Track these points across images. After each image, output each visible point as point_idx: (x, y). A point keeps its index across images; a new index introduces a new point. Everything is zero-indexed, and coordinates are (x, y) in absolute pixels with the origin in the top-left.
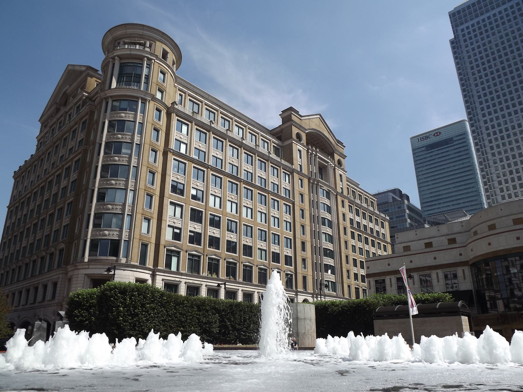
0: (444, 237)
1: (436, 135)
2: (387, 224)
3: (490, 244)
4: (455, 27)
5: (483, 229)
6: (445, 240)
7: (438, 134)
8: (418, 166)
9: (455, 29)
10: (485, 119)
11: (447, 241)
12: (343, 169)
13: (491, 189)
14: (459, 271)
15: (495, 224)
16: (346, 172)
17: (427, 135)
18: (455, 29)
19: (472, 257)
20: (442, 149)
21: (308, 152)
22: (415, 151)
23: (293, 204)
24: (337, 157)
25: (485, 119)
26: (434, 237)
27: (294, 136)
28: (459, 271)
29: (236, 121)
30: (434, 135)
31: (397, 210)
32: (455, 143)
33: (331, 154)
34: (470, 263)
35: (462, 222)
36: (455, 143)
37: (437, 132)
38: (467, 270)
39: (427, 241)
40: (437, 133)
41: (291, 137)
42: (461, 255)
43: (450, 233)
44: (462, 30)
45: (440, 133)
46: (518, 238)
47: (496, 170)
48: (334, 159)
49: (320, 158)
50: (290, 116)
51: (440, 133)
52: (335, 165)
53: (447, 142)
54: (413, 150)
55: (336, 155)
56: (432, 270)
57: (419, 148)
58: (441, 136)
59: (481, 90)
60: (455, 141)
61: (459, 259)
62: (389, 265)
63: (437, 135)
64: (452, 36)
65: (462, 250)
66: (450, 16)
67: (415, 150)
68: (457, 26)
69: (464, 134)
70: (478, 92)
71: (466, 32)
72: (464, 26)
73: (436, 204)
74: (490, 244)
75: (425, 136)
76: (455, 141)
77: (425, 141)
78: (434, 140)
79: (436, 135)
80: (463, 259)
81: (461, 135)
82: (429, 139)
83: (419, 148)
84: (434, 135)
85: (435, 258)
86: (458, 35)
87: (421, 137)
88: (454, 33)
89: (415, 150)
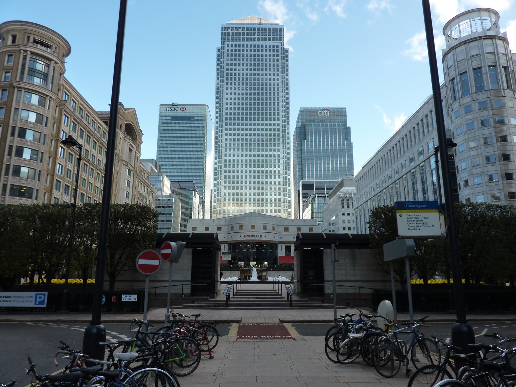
4: (224, 39)
9: (223, 41)
10: (227, 121)
11: (217, 229)
18: (223, 41)
22: (162, 117)
24: (138, 143)
25: (227, 121)
29: (87, 111)
30: (181, 109)
32: (195, 122)
36: (195, 122)
37: (183, 108)
44: (228, 46)
45: (186, 109)
49: (130, 144)
51: (186, 109)
58: (186, 111)
60: (196, 120)
67: (162, 116)
68: (225, 39)
69: (204, 117)
71: (230, 48)
72: (230, 43)
76: (196, 120)
77: (172, 111)
78: (178, 113)
80: (225, 240)
81: (201, 117)
89: (162, 116)
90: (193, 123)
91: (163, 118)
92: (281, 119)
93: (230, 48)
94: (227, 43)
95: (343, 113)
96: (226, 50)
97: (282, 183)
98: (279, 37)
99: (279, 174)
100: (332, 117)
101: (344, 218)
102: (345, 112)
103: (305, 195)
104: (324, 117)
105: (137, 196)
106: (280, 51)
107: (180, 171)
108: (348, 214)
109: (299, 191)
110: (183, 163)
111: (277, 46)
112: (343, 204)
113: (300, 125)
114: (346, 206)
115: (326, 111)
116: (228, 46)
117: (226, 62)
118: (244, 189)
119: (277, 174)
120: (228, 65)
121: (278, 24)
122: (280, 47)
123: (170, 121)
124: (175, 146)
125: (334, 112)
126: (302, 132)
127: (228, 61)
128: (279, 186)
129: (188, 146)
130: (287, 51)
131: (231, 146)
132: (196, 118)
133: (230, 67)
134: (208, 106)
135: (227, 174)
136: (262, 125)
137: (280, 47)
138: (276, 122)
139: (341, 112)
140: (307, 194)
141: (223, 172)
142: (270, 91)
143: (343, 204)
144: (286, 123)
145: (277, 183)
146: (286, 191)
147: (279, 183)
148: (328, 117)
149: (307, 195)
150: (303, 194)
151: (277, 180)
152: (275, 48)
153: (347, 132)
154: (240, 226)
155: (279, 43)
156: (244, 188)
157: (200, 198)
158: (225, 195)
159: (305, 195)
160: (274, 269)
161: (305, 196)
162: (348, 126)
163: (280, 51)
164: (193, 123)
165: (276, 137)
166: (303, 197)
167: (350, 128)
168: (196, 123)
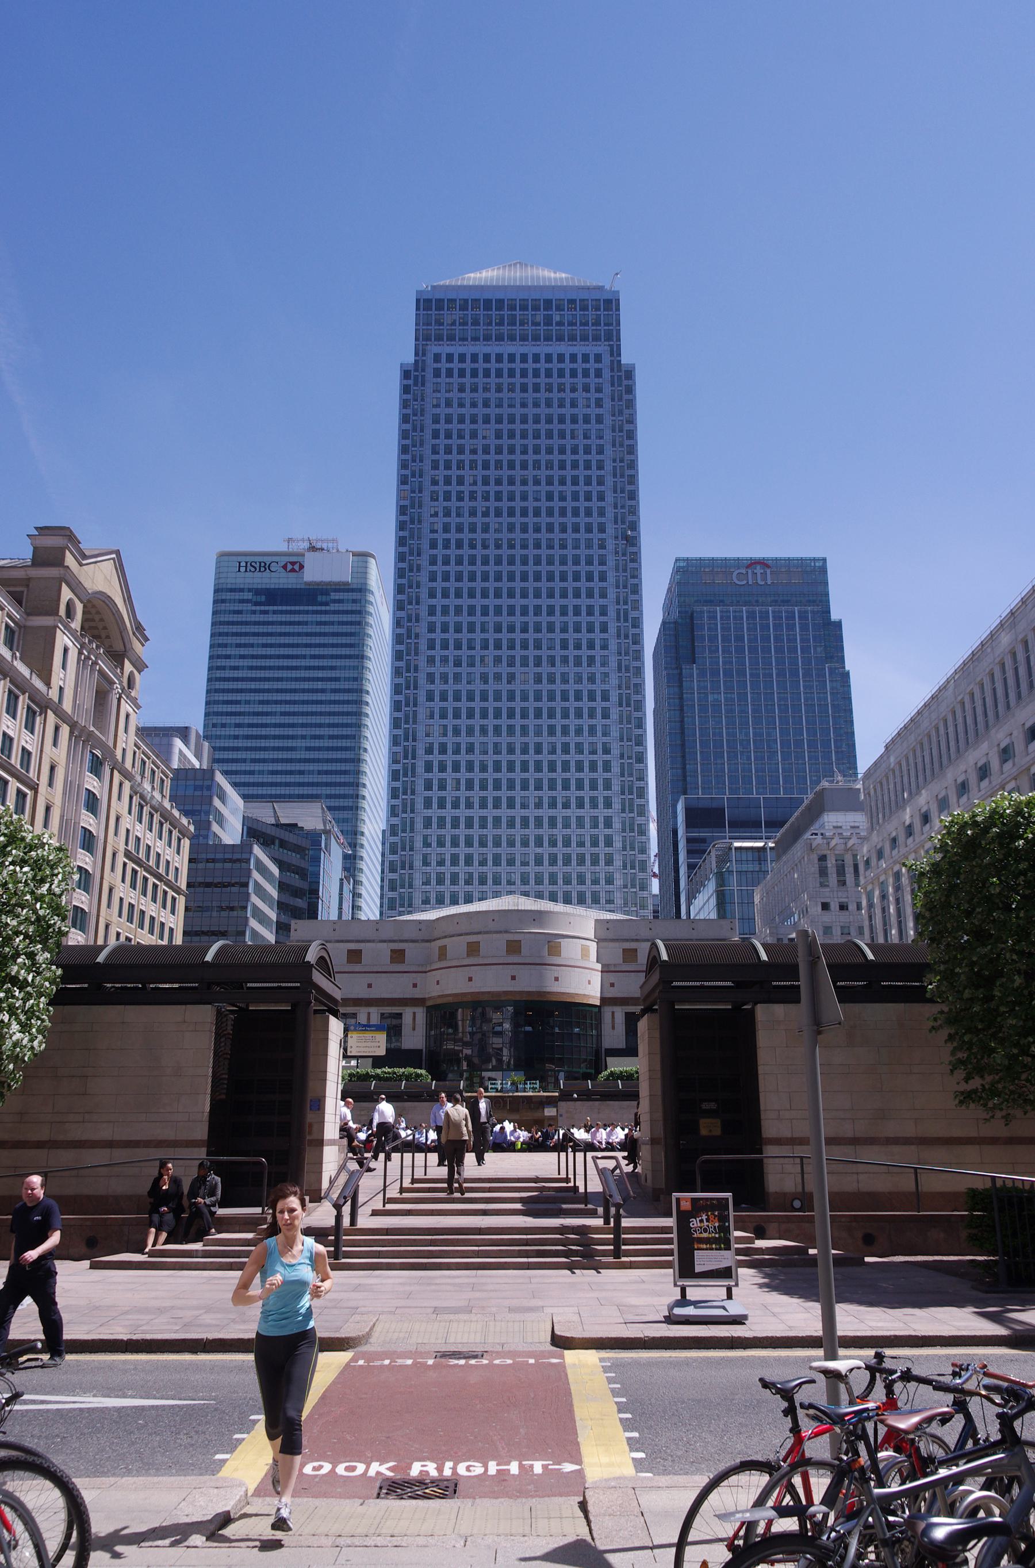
1: (290, 567)
2: (186, 843)
3: (470, 979)
4: (422, 338)
5: (457, 947)
6: (386, 949)
7: (297, 567)
8: (221, 640)
9: (421, 342)
10: (433, 602)
12: (134, 701)
13: (405, 775)
14: (408, 1013)
16: (139, 707)
17: (268, 560)
19: (434, 994)
20: (291, 612)
21: (80, 653)
22: (222, 594)
23: (35, 788)
24: (128, 667)
25: (433, 602)
26: (369, 941)
27: (62, 611)
28: (408, 1013)
30: (285, 567)
31: (190, 792)
32: (333, 607)
33: (117, 657)
34: (430, 1003)
35: (420, 922)
36: (333, 607)
38: (421, 1013)
39: (353, 946)
40: (293, 563)
41: (55, 612)
42: (415, 985)
44: (437, 358)
46: (513, 978)
47: (427, 735)
48: (122, 669)
50: (61, 552)
52: (123, 689)
53: (314, 595)
54: (217, 591)
55: (127, 663)
56: (360, 1005)
57: (232, 590)
59: (439, 527)
60: (335, 601)
61: (410, 993)
63: (293, 570)
64: (410, 358)
65: (418, 978)
66: (418, 301)
68: (427, 338)
69: (360, 590)
70: (433, 531)
72: (445, 349)
73: (244, 761)
74: (470, 979)
75: (259, 563)
76: (335, 601)
77: (257, 574)
79: (290, 567)
80: (417, 994)
81: (353, 590)
82: (267, 573)
83: (232, 590)
84: (285, 567)
85: (370, 986)
86: (424, 361)
87: (249, 559)
88: (416, 354)
90: (326, 612)
91: (228, 596)
92: (612, 594)
94: (434, 349)
96: (429, 374)
97: (617, 805)
98: (603, 328)
99: (607, 775)
101: (827, 918)
102: (823, 570)
103: (696, 846)
105: (122, 847)
106: (607, 374)
107: (279, 767)
108: (843, 907)
109: (675, 832)
110: (290, 743)
111: (598, 358)
112: (823, 872)
113: (675, 615)
114: (833, 878)
115: (759, 570)
116: (437, 358)
117: (429, 411)
118: (490, 825)
119: (600, 775)
120: (436, 420)
121: (601, 288)
122: (606, 359)
123: (251, 607)
124: (267, 685)
126: (682, 637)
127: (437, 406)
128: (608, 812)
129: (306, 685)
130: (630, 374)
131: (446, 682)
132: (334, 596)
133: (442, 427)
134: (373, 557)
135: (435, 775)
136: (551, 611)
137: (606, 359)
138: (597, 602)
140: (703, 840)
141: (420, 769)
142: (576, 504)
143: (823, 872)
144: (629, 607)
145: (601, 805)
146: (632, 830)
147: (608, 804)
149: (702, 846)
150: (689, 840)
151: (601, 794)
152: (592, 365)
153: (831, 636)
154: (470, 945)
155: (602, 348)
156: (490, 820)
157: (346, 857)
158: (427, 844)
159: (696, 846)
160: (587, 1096)
161: (697, 849)
162: (834, 616)
163: (607, 374)
164: (326, 612)
165: (598, 652)
166: (690, 852)
167: (838, 625)
168: (335, 612)
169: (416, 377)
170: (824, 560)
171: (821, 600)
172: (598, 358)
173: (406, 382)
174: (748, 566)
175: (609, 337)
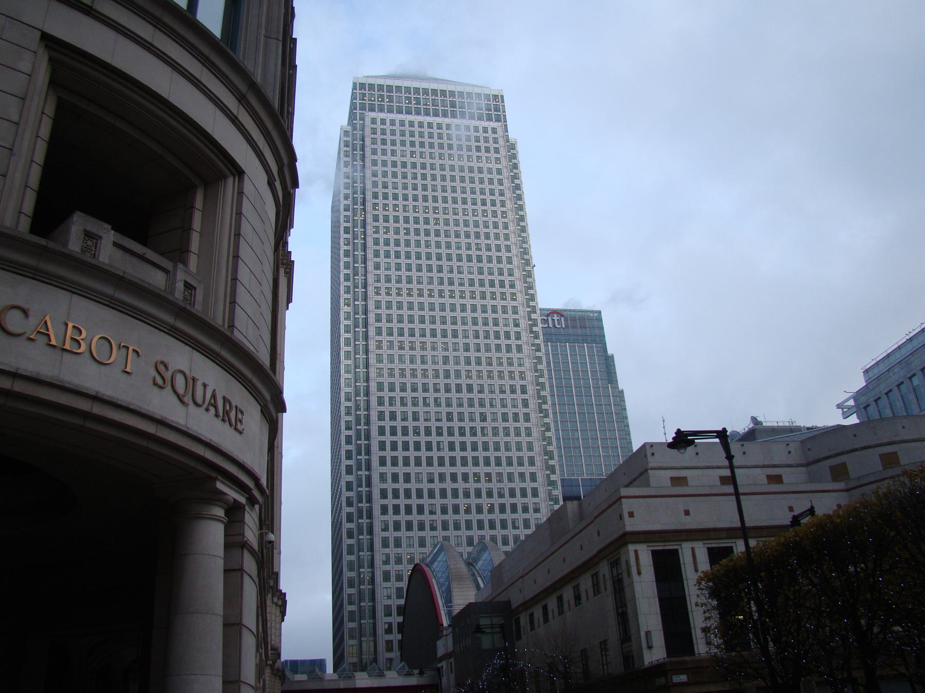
0: (759, 470)
15: (896, 453)
25: (379, 298)
43: (766, 463)
44: (374, 121)
62: (687, 513)
93: (379, 126)
95: (596, 324)
100: (571, 331)
102: (599, 319)
104: (553, 330)
115: (556, 318)
116: (374, 121)
122: (500, 132)
125: (574, 319)
137: (500, 132)
139: (591, 319)
148: (562, 331)
162: (610, 352)
167: (612, 356)
169: (353, 134)
170: (600, 312)
171: (600, 339)
172: (494, 131)
173: (346, 139)
174: (548, 315)
175: (498, 120)
